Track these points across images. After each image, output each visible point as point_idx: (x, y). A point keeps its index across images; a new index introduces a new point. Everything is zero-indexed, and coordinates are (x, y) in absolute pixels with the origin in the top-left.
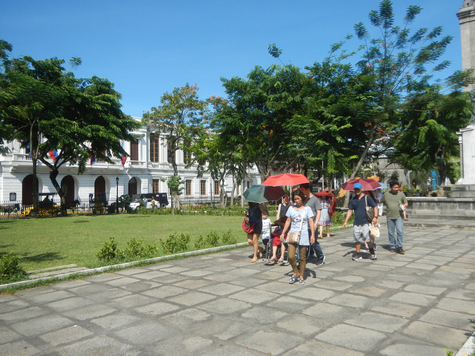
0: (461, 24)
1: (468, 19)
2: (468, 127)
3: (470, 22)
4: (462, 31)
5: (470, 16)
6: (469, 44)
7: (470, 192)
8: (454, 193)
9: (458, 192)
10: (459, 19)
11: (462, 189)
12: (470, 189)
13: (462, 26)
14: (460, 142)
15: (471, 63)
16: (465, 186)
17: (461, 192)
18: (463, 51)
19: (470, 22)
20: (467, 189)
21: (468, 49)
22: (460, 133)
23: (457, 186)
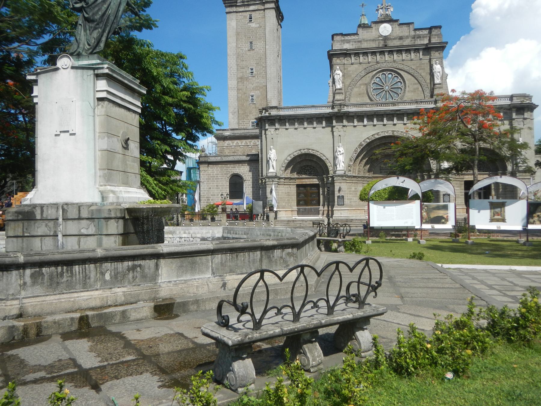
0: (227, 13)
1: (234, 9)
3: (236, 12)
4: (228, 22)
5: (236, 6)
6: (235, 38)
7: (44, 224)
8: (12, 224)
9: (20, 224)
10: (226, 7)
11: (28, 216)
12: (44, 216)
13: (228, 15)
14: (35, 100)
15: (237, 61)
16: (35, 206)
17: (26, 223)
18: (229, 46)
19: (236, 12)
20: (38, 217)
21: (234, 44)
22: (33, 77)
23: (21, 208)
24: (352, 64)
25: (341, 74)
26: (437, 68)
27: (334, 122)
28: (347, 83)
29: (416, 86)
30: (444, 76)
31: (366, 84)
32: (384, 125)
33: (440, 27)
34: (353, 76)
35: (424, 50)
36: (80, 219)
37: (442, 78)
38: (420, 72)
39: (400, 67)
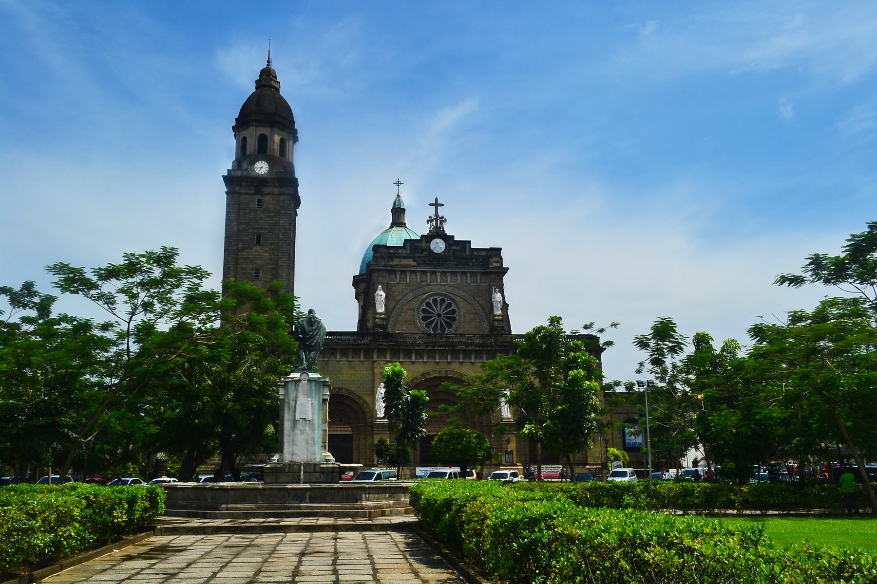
2: (292, 375)
24: (398, 283)
25: (384, 295)
26: (498, 297)
27: (375, 356)
28: (391, 307)
29: (472, 316)
30: (505, 307)
31: (414, 309)
32: (437, 363)
33: (501, 249)
34: (398, 298)
35: (482, 273)
36: (315, 472)
37: (502, 309)
38: (477, 299)
39: (456, 291)
